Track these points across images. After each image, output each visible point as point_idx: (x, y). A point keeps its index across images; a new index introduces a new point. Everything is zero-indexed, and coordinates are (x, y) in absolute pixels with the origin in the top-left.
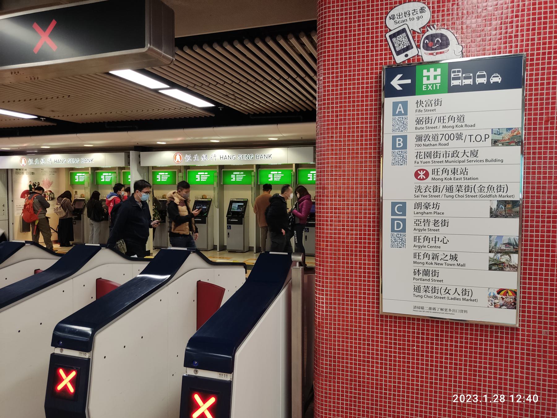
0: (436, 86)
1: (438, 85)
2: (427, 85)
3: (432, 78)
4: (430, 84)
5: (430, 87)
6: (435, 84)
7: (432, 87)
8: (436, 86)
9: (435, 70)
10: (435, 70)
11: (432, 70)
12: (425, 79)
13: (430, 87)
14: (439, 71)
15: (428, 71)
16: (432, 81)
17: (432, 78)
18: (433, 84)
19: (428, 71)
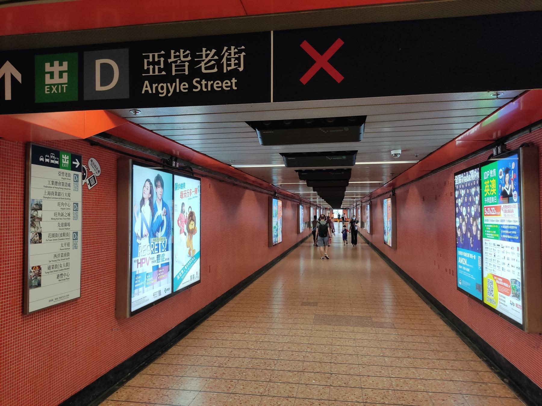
0: (62, 88)
1: (65, 86)
2: (50, 85)
3: (56, 75)
4: (54, 85)
5: (54, 89)
6: (61, 84)
7: (57, 89)
8: (62, 88)
9: (61, 64)
10: (61, 64)
11: (56, 63)
12: (47, 76)
13: (54, 89)
14: (65, 64)
15: (52, 65)
16: (57, 80)
17: (56, 75)
18: (58, 84)
19: (52, 65)
